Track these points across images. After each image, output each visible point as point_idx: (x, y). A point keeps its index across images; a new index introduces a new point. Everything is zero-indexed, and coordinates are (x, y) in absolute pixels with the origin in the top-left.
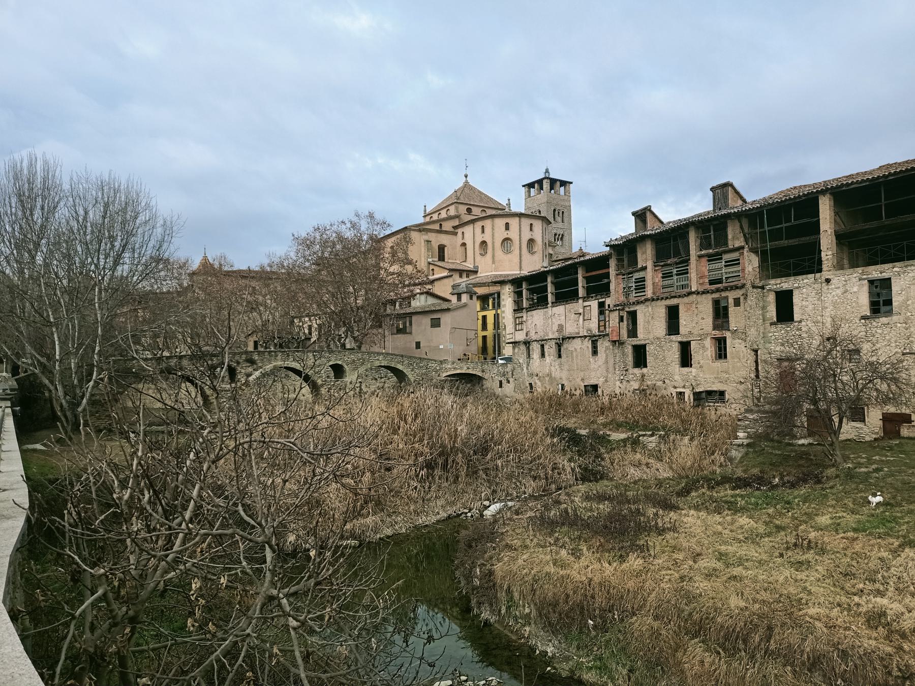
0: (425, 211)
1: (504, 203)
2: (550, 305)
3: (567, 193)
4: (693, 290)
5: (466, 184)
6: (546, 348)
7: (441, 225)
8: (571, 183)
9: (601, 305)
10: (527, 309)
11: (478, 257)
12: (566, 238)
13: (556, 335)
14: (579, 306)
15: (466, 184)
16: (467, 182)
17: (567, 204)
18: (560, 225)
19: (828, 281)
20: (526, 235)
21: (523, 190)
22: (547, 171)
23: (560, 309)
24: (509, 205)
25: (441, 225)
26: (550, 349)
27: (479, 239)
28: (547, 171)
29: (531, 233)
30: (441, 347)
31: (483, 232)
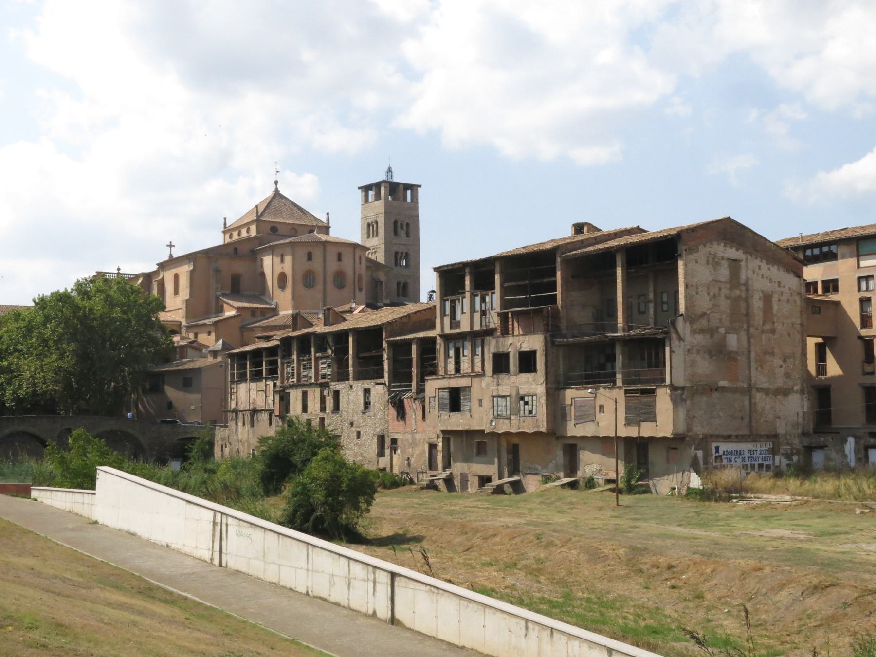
0: (225, 224)
2: (248, 380)
3: (415, 197)
4: (313, 381)
5: (277, 194)
6: (246, 417)
7: (236, 249)
8: (420, 186)
9: (275, 385)
10: (236, 381)
11: (277, 291)
13: (251, 407)
14: (261, 384)
15: (277, 194)
16: (277, 188)
19: (351, 387)
20: (333, 266)
21: (360, 194)
22: (390, 170)
23: (253, 385)
24: (328, 220)
25: (236, 249)
26: (248, 418)
27: (278, 270)
28: (390, 170)
30: (193, 407)
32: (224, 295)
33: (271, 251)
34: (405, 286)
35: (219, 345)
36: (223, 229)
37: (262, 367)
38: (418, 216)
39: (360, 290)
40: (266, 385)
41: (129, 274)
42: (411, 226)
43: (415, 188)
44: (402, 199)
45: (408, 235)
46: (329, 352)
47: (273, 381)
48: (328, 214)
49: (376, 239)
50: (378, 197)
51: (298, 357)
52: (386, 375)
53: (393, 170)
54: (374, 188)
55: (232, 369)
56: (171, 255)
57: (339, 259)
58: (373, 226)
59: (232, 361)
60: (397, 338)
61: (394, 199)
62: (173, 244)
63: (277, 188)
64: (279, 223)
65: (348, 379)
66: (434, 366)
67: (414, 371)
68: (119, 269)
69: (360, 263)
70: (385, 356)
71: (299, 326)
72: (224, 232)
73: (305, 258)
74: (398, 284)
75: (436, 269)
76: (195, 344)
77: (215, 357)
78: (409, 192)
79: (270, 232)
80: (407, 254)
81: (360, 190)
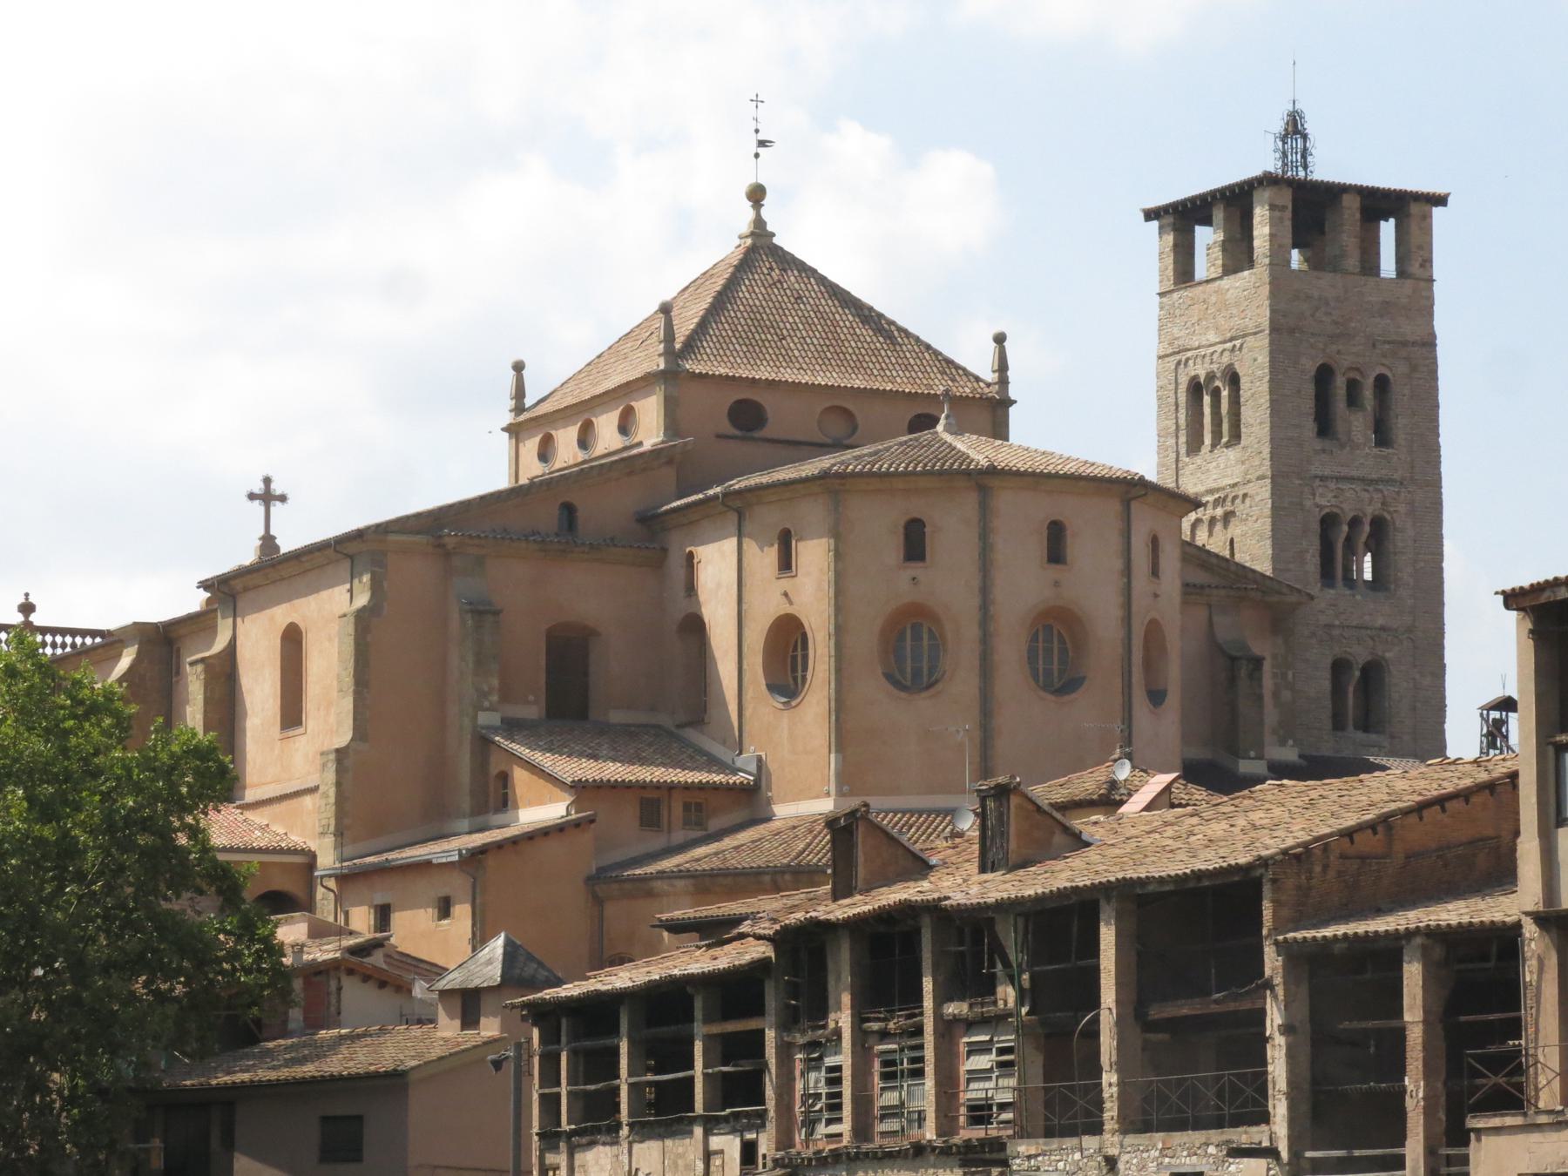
0: (519, 393)
2: (625, 1131)
4: (929, 1133)
8: (1441, 200)
9: (749, 1153)
11: (763, 709)
12: (1402, 539)
14: (689, 1148)
18: (1363, 456)
19: (1111, 1162)
21: (1152, 242)
22: (1294, 128)
24: (1002, 367)
25: (569, 510)
27: (767, 607)
28: (1294, 128)
29: (1053, 571)
32: (512, 727)
33: (734, 517)
34: (1373, 674)
35: (489, 962)
36: (508, 418)
37: (691, 1066)
38: (1429, 343)
39: (1156, 697)
40: (708, 1156)
41: (74, 632)
42: (1400, 393)
43: (1415, 209)
44: (1352, 262)
45: (1382, 435)
46: (1007, 994)
47: (740, 1132)
48: (1000, 339)
49: (1232, 454)
50: (1238, 255)
51: (859, 1020)
52: (1279, 1109)
53: (1310, 127)
54: (1218, 215)
55: (550, 1075)
56: (268, 542)
58: (1216, 394)
59: (550, 1037)
60: (1328, 932)
61: (1316, 263)
62: (277, 488)
63: (759, 223)
64: (771, 384)
65: (1096, 1129)
66: (1514, 1065)
67: (1414, 1085)
68: (27, 608)
69: (1155, 572)
70: (1274, 1017)
71: (861, 872)
72: (515, 431)
73: (892, 549)
74: (1339, 668)
75: (1513, 599)
76: (377, 959)
77: (469, 1020)
78: (1387, 229)
79: (727, 428)
80: (1379, 525)
81: (1155, 224)
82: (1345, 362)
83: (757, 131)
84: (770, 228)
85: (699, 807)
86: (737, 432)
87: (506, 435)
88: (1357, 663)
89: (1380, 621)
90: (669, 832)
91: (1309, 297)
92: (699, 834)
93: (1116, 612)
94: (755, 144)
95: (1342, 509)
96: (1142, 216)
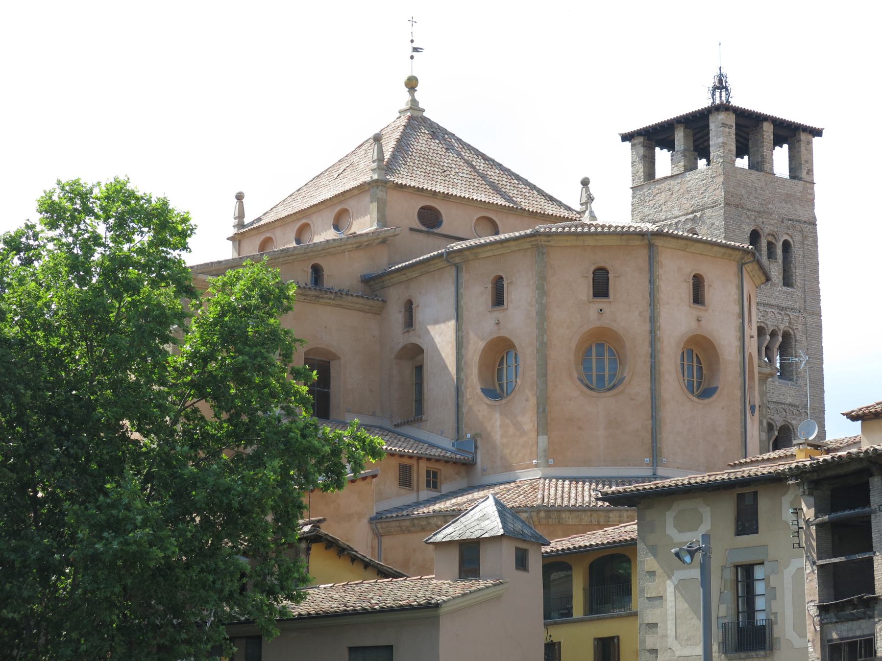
0: (241, 215)
1: (572, 198)
7: (317, 271)
8: (818, 133)
17: (804, 216)
22: (721, 85)
25: (317, 271)
28: (721, 85)
29: (697, 310)
31: (498, 300)
33: (453, 271)
36: (232, 232)
38: (812, 223)
42: (797, 252)
43: (803, 136)
45: (787, 281)
53: (731, 83)
54: (679, 137)
57: (698, 297)
64: (447, 197)
69: (750, 320)
73: (585, 288)
79: (417, 224)
81: (628, 144)
82: (766, 229)
83: (412, 41)
84: (421, 106)
85: (435, 474)
86: (424, 229)
87: (231, 243)
88: (777, 426)
89: (789, 400)
90: (418, 491)
91: (745, 186)
92: (435, 494)
93: (736, 343)
94: (411, 50)
95: (766, 324)
96: (620, 138)
